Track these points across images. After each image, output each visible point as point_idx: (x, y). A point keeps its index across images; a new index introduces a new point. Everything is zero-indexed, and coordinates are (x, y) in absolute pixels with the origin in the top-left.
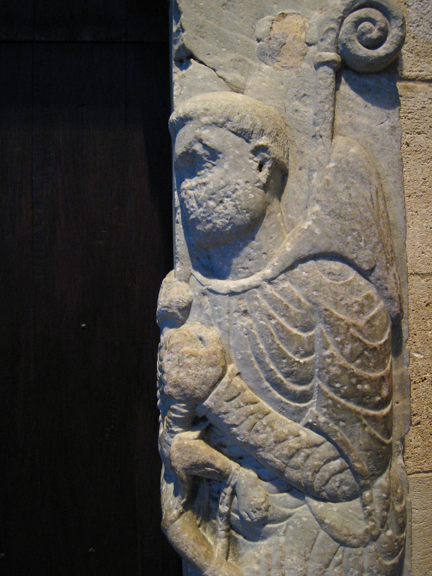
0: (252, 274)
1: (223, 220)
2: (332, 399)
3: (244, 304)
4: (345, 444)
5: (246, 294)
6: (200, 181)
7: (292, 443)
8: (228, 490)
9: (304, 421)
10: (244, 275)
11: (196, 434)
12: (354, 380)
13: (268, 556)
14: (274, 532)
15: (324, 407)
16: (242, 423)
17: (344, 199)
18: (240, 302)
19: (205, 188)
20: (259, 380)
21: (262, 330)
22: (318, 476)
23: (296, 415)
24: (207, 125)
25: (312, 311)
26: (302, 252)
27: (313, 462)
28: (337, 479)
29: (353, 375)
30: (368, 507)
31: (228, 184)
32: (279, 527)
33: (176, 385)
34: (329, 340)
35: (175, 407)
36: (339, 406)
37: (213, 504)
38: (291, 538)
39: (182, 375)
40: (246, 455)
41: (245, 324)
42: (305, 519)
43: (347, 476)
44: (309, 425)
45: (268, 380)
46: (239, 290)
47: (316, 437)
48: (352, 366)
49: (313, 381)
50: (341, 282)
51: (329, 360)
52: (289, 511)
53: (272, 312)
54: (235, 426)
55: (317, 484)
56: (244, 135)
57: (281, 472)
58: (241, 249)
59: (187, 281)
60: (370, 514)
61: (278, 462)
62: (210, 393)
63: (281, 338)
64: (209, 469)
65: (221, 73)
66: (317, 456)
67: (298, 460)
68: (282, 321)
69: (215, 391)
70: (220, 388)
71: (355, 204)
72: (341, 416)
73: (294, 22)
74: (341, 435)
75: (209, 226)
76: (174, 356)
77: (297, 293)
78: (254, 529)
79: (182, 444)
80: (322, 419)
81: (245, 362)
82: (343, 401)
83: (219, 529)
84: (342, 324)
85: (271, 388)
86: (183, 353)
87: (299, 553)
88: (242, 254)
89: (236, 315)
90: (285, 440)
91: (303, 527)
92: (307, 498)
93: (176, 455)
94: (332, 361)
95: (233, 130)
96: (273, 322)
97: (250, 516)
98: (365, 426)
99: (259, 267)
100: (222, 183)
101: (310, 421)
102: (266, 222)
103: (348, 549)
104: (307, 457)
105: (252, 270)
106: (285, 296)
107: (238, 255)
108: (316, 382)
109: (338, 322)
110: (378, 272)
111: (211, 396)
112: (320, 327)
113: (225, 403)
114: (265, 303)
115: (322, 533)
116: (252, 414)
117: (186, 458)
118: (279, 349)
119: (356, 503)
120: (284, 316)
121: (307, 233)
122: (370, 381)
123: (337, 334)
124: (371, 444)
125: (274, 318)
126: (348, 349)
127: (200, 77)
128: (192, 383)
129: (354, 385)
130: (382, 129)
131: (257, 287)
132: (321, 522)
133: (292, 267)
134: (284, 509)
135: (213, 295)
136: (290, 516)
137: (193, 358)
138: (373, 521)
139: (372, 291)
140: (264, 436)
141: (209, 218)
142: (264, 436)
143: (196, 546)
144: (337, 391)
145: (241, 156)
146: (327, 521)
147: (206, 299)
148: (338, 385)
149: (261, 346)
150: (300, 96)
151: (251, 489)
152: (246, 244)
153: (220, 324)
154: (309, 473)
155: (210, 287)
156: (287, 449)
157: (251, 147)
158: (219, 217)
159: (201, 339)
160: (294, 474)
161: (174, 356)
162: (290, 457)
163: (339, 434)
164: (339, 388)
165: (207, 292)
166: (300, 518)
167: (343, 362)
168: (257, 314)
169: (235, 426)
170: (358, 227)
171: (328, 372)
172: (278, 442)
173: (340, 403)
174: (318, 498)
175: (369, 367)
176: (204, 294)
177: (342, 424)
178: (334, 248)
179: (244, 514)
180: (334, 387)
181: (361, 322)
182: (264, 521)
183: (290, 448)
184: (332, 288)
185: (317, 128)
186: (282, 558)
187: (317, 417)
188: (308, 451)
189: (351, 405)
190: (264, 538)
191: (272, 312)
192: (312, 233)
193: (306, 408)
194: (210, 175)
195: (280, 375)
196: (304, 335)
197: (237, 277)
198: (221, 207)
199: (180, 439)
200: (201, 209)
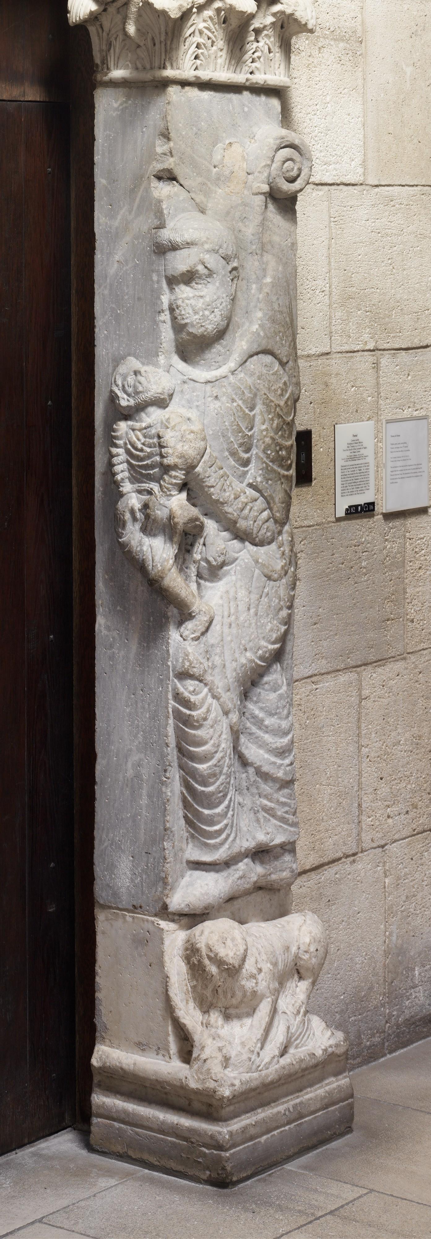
0: (220, 367)
2: (266, 463)
5: (217, 382)
6: (197, 294)
7: (243, 499)
8: (202, 541)
9: (246, 482)
12: (278, 448)
13: (227, 592)
14: (227, 573)
18: (213, 389)
19: (201, 300)
24: (208, 251)
27: (254, 513)
28: (265, 527)
29: (278, 444)
30: (282, 549)
32: (231, 569)
33: (182, 456)
34: (266, 416)
38: (239, 576)
39: (185, 448)
42: (246, 561)
44: (250, 485)
47: (256, 494)
50: (271, 372)
52: (236, 555)
54: (213, 487)
60: (283, 554)
64: (197, 523)
67: (246, 511)
69: (203, 460)
70: (206, 457)
72: (271, 476)
75: (201, 330)
76: (177, 434)
82: (271, 464)
83: (193, 575)
84: (273, 404)
85: (229, 457)
88: (214, 350)
89: (210, 399)
91: (246, 567)
92: (247, 543)
93: (180, 512)
96: (235, 404)
97: (215, 560)
98: (282, 483)
99: (225, 361)
100: (215, 297)
101: (251, 481)
103: (272, 583)
104: (251, 509)
105: (220, 364)
106: (242, 384)
111: (201, 464)
120: (241, 399)
123: (270, 413)
125: (236, 401)
129: (278, 452)
130: (286, 245)
133: (245, 361)
134: (234, 554)
137: (192, 434)
140: (227, 494)
141: (203, 324)
142: (227, 494)
147: (186, 386)
148: (269, 452)
150: (242, 218)
151: (215, 539)
154: (252, 522)
155: (190, 377)
156: (240, 504)
157: (229, 268)
158: (210, 323)
160: (242, 524)
161: (177, 434)
162: (242, 510)
164: (269, 455)
165: (188, 381)
166: (243, 560)
168: (224, 398)
169: (213, 487)
171: (264, 442)
172: (236, 498)
175: (285, 437)
177: (270, 482)
179: (211, 559)
180: (267, 454)
181: (282, 403)
182: (223, 564)
183: (243, 502)
186: (236, 592)
189: (275, 467)
190: (220, 579)
192: (259, 334)
193: (247, 471)
194: (206, 290)
198: (213, 315)
200: (197, 317)
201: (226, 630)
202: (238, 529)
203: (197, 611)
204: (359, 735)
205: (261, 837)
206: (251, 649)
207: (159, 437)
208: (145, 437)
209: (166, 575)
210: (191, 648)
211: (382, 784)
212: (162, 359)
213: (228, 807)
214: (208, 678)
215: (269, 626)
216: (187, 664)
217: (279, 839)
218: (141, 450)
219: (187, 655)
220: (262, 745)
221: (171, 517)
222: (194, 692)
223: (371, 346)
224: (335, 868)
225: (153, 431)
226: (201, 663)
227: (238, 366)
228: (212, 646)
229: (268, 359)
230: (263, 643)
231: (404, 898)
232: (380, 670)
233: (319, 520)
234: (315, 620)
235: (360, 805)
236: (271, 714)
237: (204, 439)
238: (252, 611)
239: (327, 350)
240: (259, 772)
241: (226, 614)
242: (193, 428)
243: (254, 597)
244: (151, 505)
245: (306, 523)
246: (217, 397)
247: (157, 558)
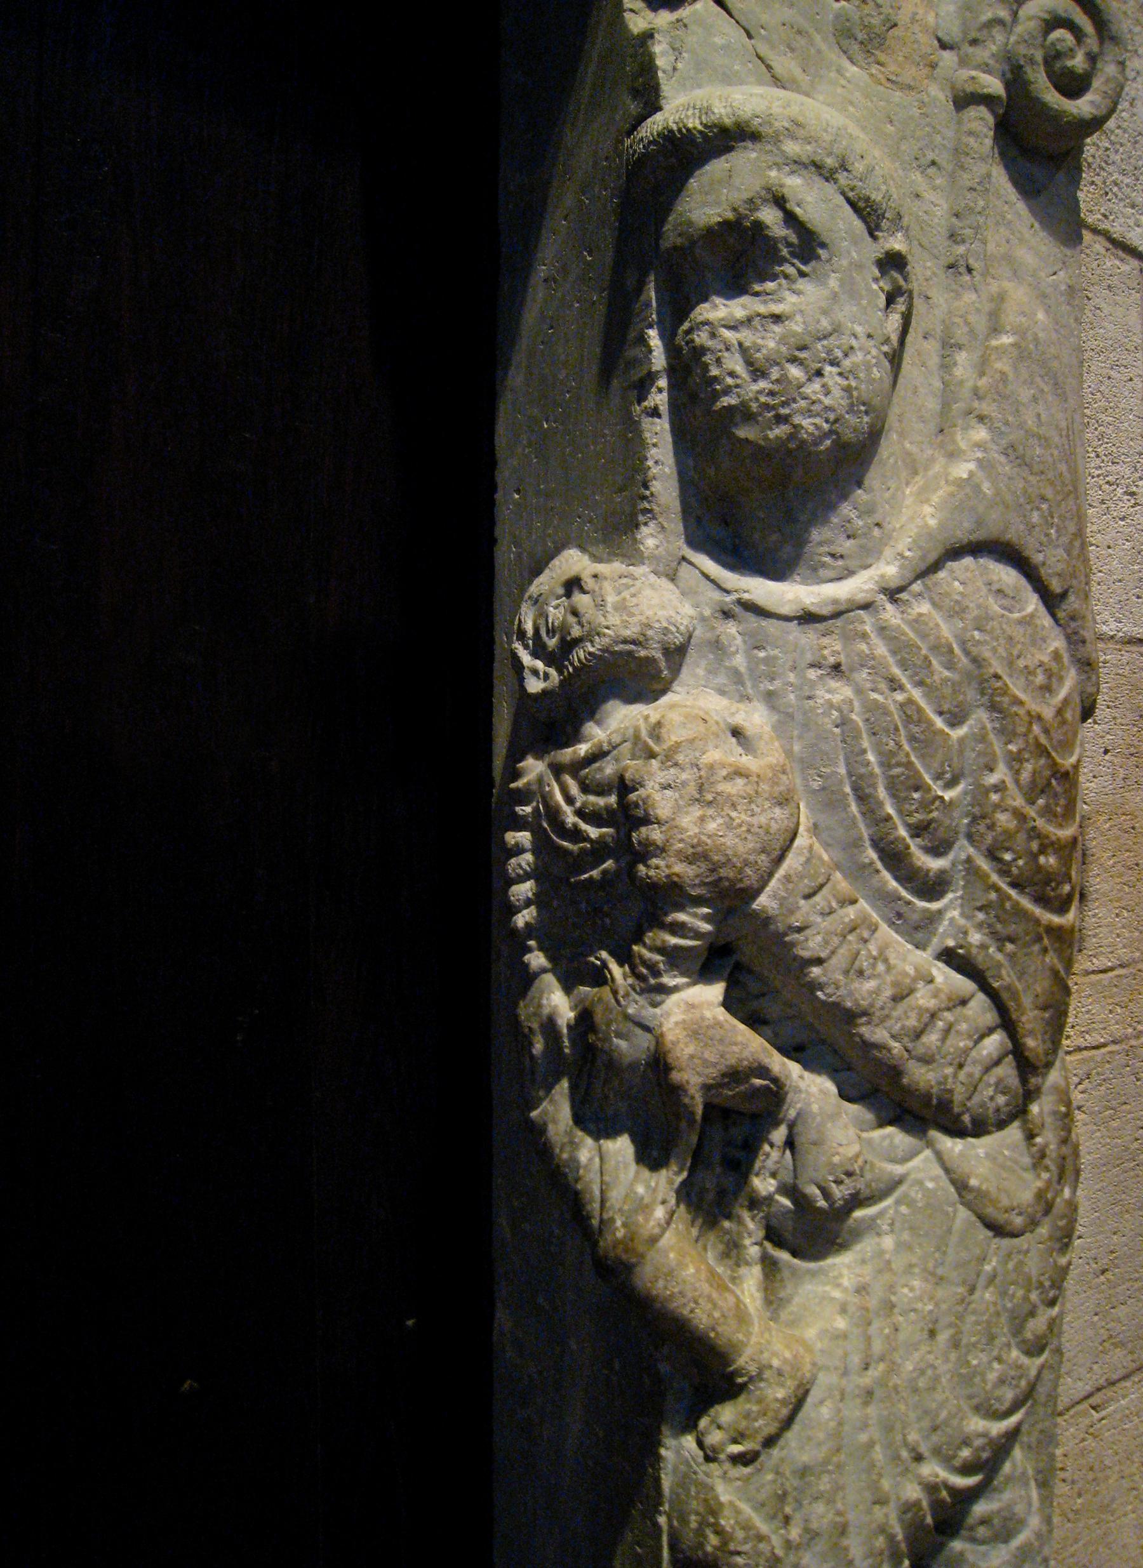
0: (851, 573)
1: (817, 420)
3: (833, 648)
4: (1015, 995)
5: (839, 622)
6: (762, 309)
7: (923, 998)
8: (779, 1135)
9: (936, 944)
10: (832, 574)
11: (715, 991)
12: (1035, 846)
13: (861, 1289)
14: (870, 1226)
15: (980, 909)
16: (833, 952)
17: (1030, 422)
18: (825, 641)
19: (777, 329)
20: (857, 844)
22: (962, 1075)
23: (918, 930)
24: (798, 165)
25: (968, 675)
26: (959, 533)
28: (992, 1080)
29: (1034, 833)
31: (837, 330)
32: (881, 1214)
33: (698, 855)
34: (997, 746)
35: (682, 917)
36: (1008, 905)
37: (729, 1182)
38: (906, 1236)
39: (712, 826)
40: (829, 1038)
41: (836, 698)
42: (930, 1185)
43: (1007, 1071)
44: (948, 957)
45: (875, 844)
46: (825, 611)
48: (1031, 812)
49: (956, 846)
50: (1016, 615)
51: (995, 797)
52: (898, 1169)
53: (896, 671)
54: (819, 961)
57: (895, 1072)
58: (832, 507)
59: (673, 578)
61: (896, 1046)
62: (771, 875)
63: (912, 739)
64: (758, 1082)
65: (764, 50)
66: (964, 1026)
67: (932, 1038)
68: (917, 694)
70: (792, 862)
71: (1046, 440)
72: (1012, 929)
74: (1005, 977)
75: (779, 432)
76: (684, 776)
77: (947, 631)
78: (813, 1229)
80: (975, 938)
81: (829, 800)
82: (1013, 893)
83: (747, 1242)
84: (1022, 712)
85: (879, 865)
86: (711, 767)
87: (925, 1270)
89: (812, 674)
90: (911, 991)
91: (928, 1205)
92: (934, 1134)
93: (690, 1049)
94: (1002, 799)
95: (851, 194)
96: (900, 697)
99: (867, 556)
100: (825, 324)
101: (951, 943)
103: (1006, 1242)
104: (947, 1031)
105: (852, 563)
106: (924, 636)
107: (826, 521)
108: (963, 849)
109: (1015, 709)
111: (773, 883)
112: (981, 717)
113: (802, 902)
114: (881, 650)
115: (963, 1213)
116: (852, 930)
117: (710, 1055)
118: (909, 765)
119: (1014, 1132)
120: (920, 684)
121: (968, 490)
124: (1053, 993)
125: (901, 688)
127: (718, 41)
128: (741, 849)
129: (1035, 857)
130: (1055, 287)
131: (866, 606)
132: (961, 1186)
133: (935, 567)
135: (751, 618)
136: (899, 1181)
137: (740, 782)
138: (1047, 1169)
139: (1057, 643)
140: (871, 985)
141: (784, 411)
142: (871, 985)
143: (715, 1295)
144: (1004, 872)
145: (860, 267)
146: (973, 1182)
149: (871, 757)
150: (923, 161)
152: (844, 497)
153: (770, 697)
154: (949, 1071)
155: (746, 596)
156: (913, 1015)
158: (809, 413)
159: (736, 732)
160: (921, 1076)
162: (918, 1035)
163: (1004, 972)
164: (1009, 864)
165: (737, 609)
166: (920, 1183)
167: (1019, 802)
168: (864, 674)
169: (819, 961)
170: (1049, 493)
171: (991, 827)
172: (897, 999)
173: (1009, 898)
174: (957, 1131)
175: (1055, 816)
176: (727, 614)
177: (1009, 947)
178: (1010, 536)
179: (813, 1191)
181: (1048, 713)
182: (857, 1201)
183: (921, 1010)
184: (1004, 626)
185: (961, 249)
187: (966, 933)
188: (947, 1015)
189: (1026, 903)
190: (843, 1247)
191: (896, 671)
192: (977, 488)
193: (940, 912)
194: (792, 299)
195: (903, 832)
197: (815, 576)
199: (691, 1006)
200: (762, 384)
201: (853, 1411)
202: (908, 1091)
203: (753, 1369)
206: (937, 1452)
207: (624, 786)
208: (585, 789)
209: (642, 1256)
210: (727, 1490)
212: (649, 538)
216: (714, 1539)
218: (576, 835)
219: (714, 1513)
221: (659, 1063)
225: (608, 769)
226: (760, 1538)
227: (909, 576)
228: (804, 1472)
229: (1007, 575)
230: (977, 1424)
233: (1117, 1030)
234: (1104, 1262)
237: (784, 800)
238: (943, 1337)
241: (856, 1360)
242: (747, 761)
244: (599, 1017)
245: (1090, 1040)
246: (837, 667)
247: (616, 1196)
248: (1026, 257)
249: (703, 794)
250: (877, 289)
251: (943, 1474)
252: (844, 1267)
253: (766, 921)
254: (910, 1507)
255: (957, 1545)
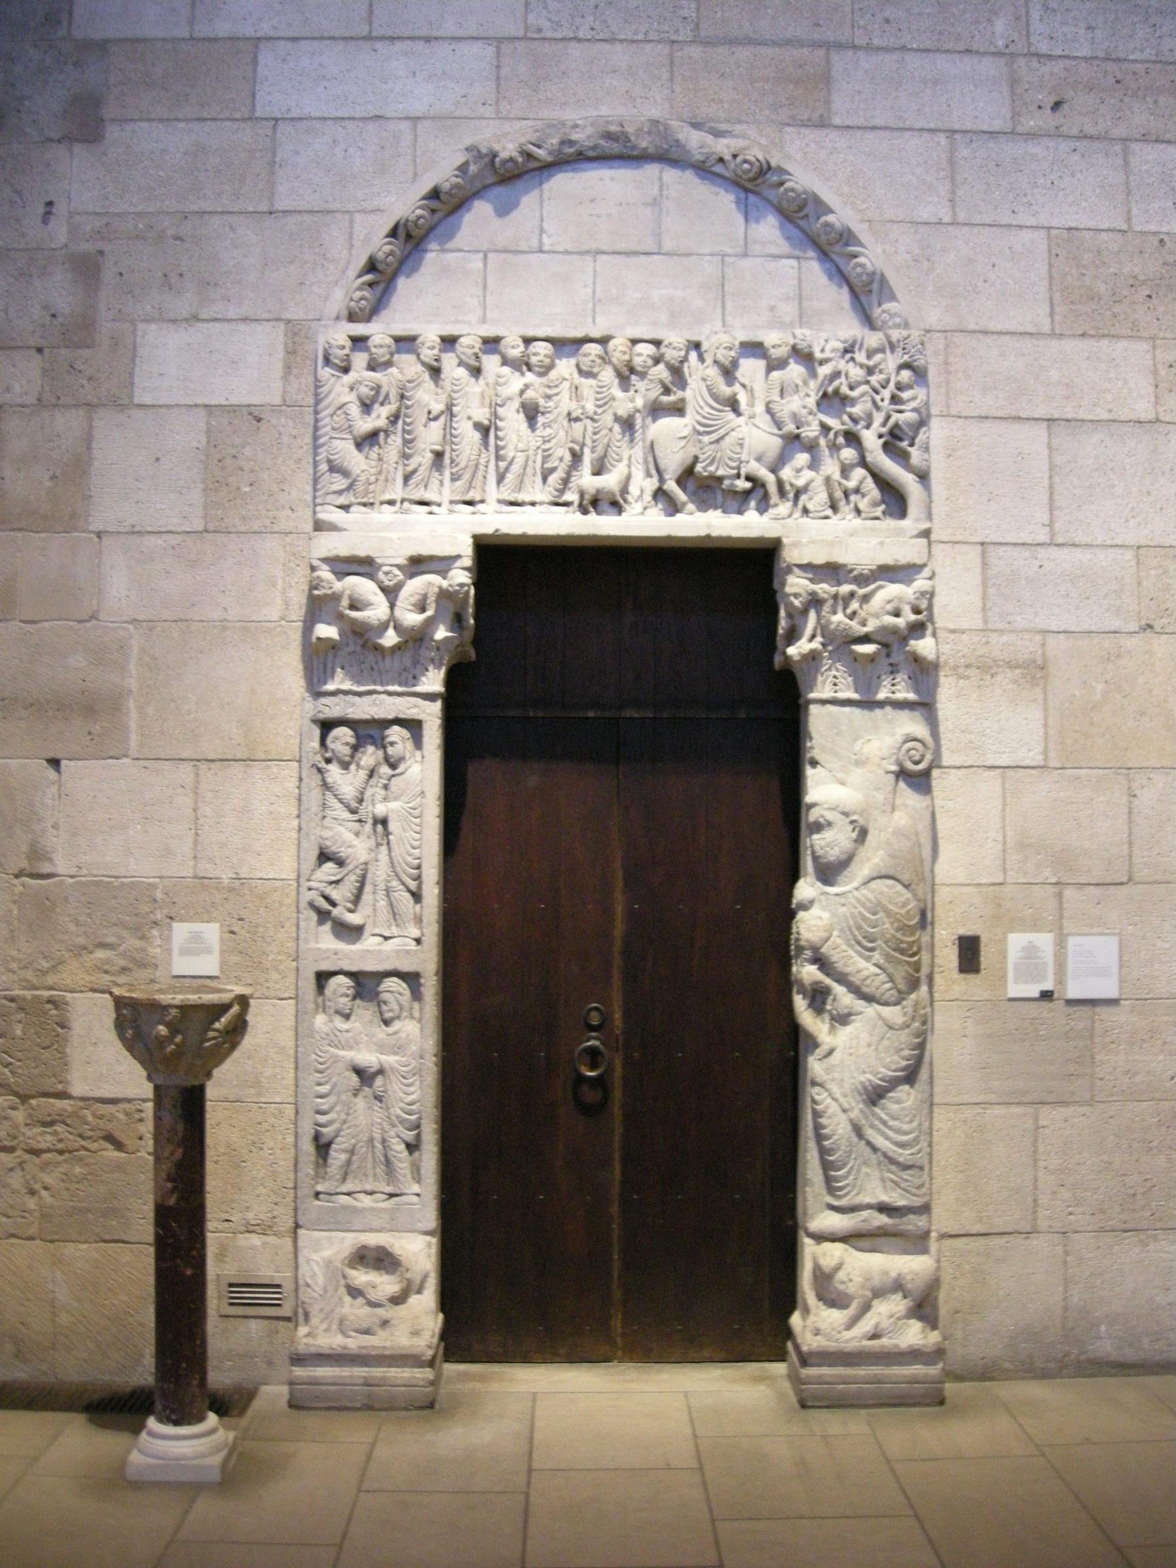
3: (842, 901)
7: (866, 973)
14: (853, 1021)
21: (852, 913)
23: (868, 959)
27: (876, 983)
29: (898, 939)
40: (842, 979)
43: (894, 992)
44: (875, 965)
47: (878, 971)
55: (878, 996)
56: (846, 814)
67: (868, 982)
68: (862, 910)
70: (829, 943)
73: (875, 744)
74: (891, 970)
77: (870, 896)
79: (807, 972)
81: (842, 931)
99: (851, 882)
102: (856, 859)
108: (879, 942)
110: (913, 886)
112: (881, 914)
114: (853, 901)
119: (898, 1008)
122: (907, 942)
126: (896, 925)
133: (868, 882)
151: (843, 997)
160: (865, 990)
167: (893, 932)
181: (903, 911)
196: (874, 918)
197: (839, 886)
204: (1035, 1152)
205: (884, 1198)
211: (1063, 1189)
213: (849, 1173)
214: (828, 1086)
215: (889, 1060)
217: (901, 1203)
220: (887, 1138)
222: (818, 1094)
223: (1054, 880)
224: (1006, 1238)
230: (883, 1070)
231: (1088, 1273)
232: (1062, 1109)
235: (1035, 1200)
236: (894, 1118)
239: (1001, 880)
240: (885, 1155)
243: (875, 1039)
248: (910, 802)
249: (809, 930)
250: (850, 828)
251: (872, 1078)
252: (849, 1029)
253: (822, 954)
254: (861, 1082)
255: (883, 1101)
